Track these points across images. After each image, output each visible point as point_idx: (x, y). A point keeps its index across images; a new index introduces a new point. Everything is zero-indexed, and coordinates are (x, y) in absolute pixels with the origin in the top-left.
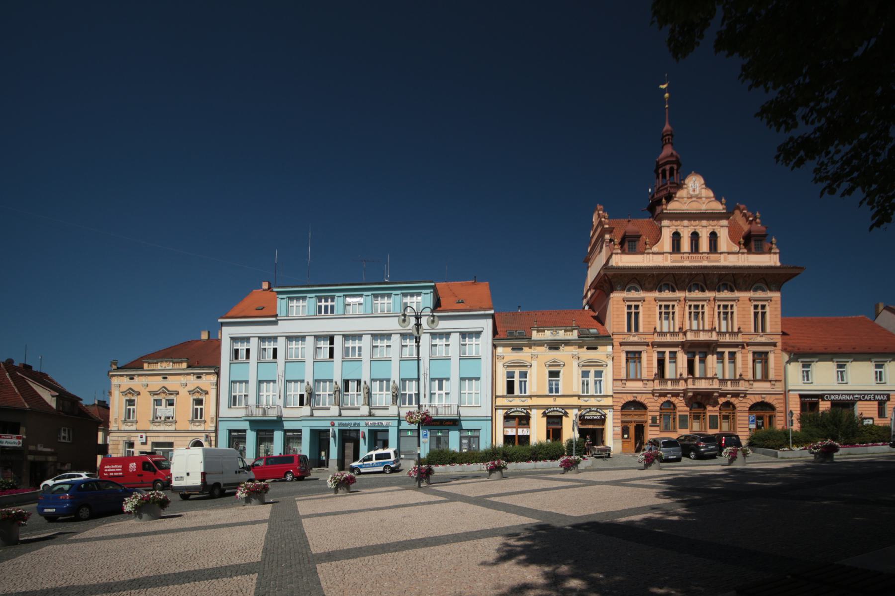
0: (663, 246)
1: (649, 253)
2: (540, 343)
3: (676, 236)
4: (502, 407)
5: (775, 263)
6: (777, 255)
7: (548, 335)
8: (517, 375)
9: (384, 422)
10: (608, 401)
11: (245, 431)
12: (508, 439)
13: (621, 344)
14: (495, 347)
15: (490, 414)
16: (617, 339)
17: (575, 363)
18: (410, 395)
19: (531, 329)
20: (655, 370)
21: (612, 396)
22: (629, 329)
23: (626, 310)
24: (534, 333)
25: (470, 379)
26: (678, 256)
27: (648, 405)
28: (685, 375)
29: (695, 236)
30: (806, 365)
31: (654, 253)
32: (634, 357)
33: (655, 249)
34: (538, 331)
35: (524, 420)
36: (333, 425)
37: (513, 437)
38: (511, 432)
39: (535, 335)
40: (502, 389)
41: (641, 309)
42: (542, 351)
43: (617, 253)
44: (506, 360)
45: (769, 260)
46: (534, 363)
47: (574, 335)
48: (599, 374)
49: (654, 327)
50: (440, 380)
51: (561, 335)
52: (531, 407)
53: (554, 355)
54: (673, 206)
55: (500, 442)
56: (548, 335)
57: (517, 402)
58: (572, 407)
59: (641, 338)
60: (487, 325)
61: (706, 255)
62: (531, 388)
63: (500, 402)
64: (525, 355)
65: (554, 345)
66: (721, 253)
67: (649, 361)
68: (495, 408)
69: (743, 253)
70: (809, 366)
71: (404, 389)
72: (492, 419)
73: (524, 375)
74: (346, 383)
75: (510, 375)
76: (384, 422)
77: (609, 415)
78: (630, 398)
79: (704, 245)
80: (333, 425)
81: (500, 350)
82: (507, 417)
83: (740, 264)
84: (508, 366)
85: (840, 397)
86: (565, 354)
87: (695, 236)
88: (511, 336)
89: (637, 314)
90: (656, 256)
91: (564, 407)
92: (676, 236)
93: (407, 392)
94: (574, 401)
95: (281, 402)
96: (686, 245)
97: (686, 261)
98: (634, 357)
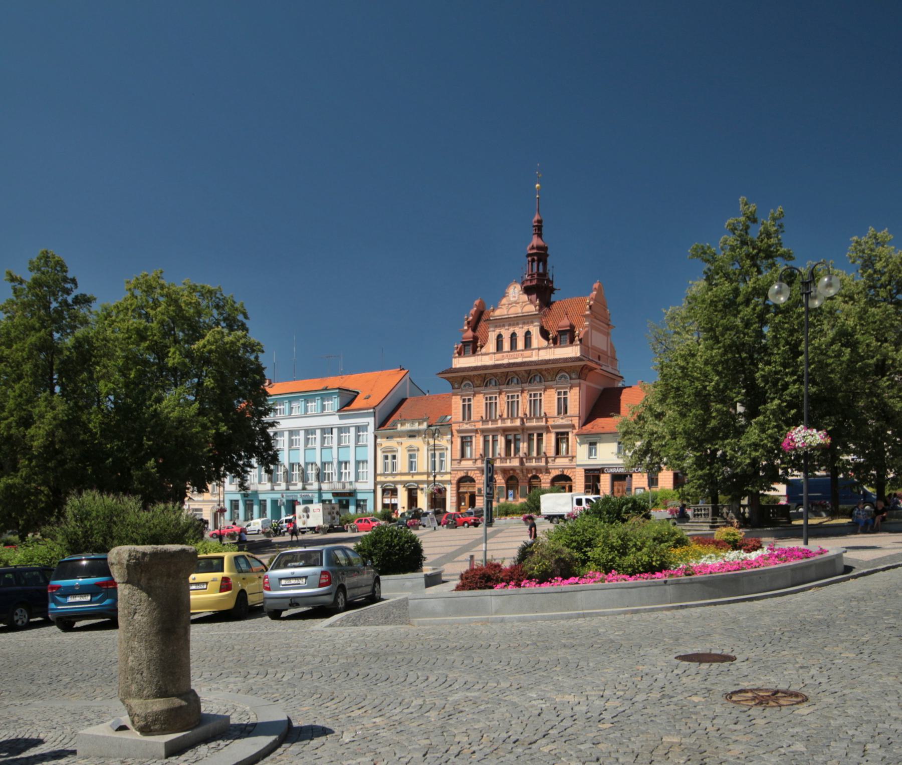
0: (489, 348)
1: (478, 355)
3: (499, 338)
4: (382, 483)
5: (576, 354)
6: (579, 347)
7: (408, 427)
8: (390, 457)
9: (310, 495)
10: (447, 477)
11: (238, 501)
12: (385, 506)
13: (459, 431)
14: (376, 437)
15: (373, 488)
16: (455, 427)
17: (426, 448)
18: (329, 474)
20: (481, 452)
21: (450, 473)
22: (464, 419)
23: (461, 403)
24: (399, 425)
26: (499, 355)
27: (476, 479)
28: (503, 455)
29: (513, 336)
30: (593, 444)
31: (482, 355)
32: (465, 442)
33: (484, 350)
34: (402, 425)
35: (394, 492)
36: (283, 496)
37: (388, 504)
38: (387, 501)
41: (472, 403)
43: (455, 357)
44: (383, 446)
45: (572, 351)
46: (399, 449)
47: (424, 426)
48: (442, 455)
49: (480, 415)
50: (346, 463)
51: (416, 426)
52: (396, 483)
54: (499, 313)
55: (379, 508)
56: (408, 427)
57: (390, 479)
58: (422, 482)
59: (471, 426)
60: (371, 421)
61: (521, 352)
62: (399, 469)
63: (379, 479)
65: (412, 435)
66: (533, 349)
67: (478, 442)
68: (376, 484)
69: (551, 348)
70: (595, 444)
71: (325, 469)
72: (375, 491)
73: (394, 457)
74: (292, 465)
75: (386, 458)
76: (310, 495)
77: (448, 487)
78: (462, 474)
79: (520, 344)
80: (283, 496)
82: (384, 491)
83: (552, 357)
84: (384, 452)
85: (618, 470)
86: (417, 442)
87: (513, 336)
89: (469, 406)
90: (484, 357)
91: (416, 482)
92: (499, 338)
93: (327, 472)
94: (424, 478)
95: (256, 480)
96: (506, 346)
97: (505, 359)
98: (465, 442)
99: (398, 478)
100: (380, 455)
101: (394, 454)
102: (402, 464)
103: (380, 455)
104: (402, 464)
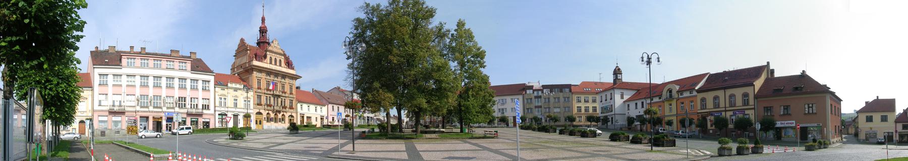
2: (231, 88)
4: (218, 111)
7: (234, 85)
8: (223, 99)
19: (228, 82)
25: (206, 99)
39: (229, 85)
40: (217, 104)
42: (231, 91)
53: (236, 93)
57: (223, 109)
64: (225, 92)
65: (236, 90)
68: (215, 111)
73: (225, 99)
81: (217, 89)
86: (239, 92)
88: (221, 85)
99: (229, 109)
100: (217, 98)
101: (225, 97)
102: (230, 102)
103: (217, 98)
104: (230, 102)
